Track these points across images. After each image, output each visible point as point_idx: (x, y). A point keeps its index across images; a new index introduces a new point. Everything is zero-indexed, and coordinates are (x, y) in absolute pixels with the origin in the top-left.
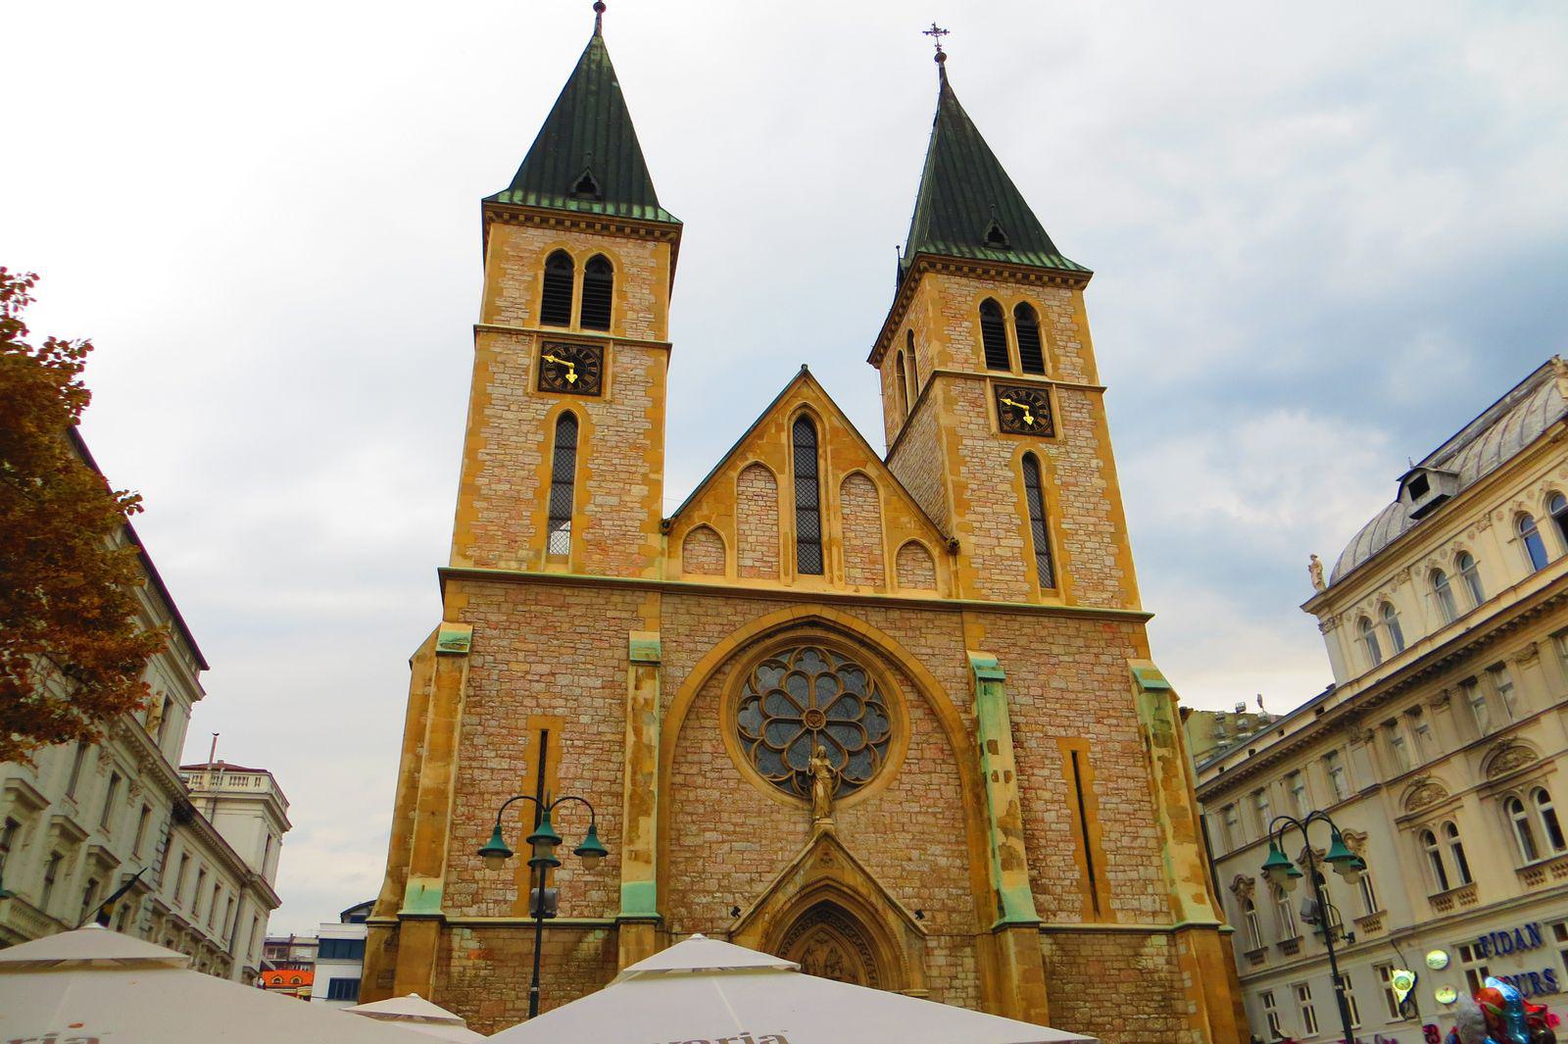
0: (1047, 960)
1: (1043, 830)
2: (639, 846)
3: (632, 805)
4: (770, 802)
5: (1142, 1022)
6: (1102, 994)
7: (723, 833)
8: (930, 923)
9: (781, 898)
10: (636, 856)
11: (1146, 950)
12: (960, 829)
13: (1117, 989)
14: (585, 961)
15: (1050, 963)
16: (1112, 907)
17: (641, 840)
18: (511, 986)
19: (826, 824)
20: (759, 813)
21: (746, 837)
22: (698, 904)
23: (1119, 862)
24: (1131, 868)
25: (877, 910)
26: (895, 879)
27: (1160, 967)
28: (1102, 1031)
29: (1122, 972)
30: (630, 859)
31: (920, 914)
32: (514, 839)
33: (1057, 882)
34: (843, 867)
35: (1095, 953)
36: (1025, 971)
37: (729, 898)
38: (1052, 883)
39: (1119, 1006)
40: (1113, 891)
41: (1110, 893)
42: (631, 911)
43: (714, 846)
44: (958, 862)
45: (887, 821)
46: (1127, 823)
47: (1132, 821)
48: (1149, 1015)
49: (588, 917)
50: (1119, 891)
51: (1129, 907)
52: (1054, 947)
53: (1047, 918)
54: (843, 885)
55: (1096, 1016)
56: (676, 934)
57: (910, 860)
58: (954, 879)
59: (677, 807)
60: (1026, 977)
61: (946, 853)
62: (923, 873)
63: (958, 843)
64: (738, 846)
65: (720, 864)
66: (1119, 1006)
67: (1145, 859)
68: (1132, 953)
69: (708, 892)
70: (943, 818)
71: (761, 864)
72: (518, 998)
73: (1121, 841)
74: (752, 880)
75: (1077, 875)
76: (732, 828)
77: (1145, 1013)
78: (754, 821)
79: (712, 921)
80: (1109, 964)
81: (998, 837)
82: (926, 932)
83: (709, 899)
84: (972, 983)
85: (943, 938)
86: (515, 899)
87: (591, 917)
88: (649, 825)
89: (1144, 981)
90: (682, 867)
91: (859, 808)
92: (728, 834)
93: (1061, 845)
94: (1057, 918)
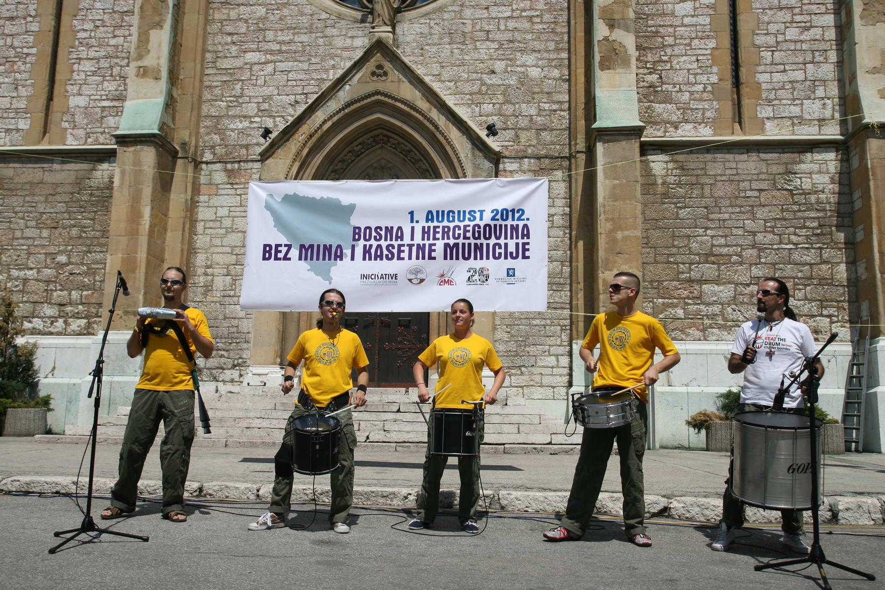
0: (660, 181)
1: (671, 26)
2: (149, 61)
3: (142, 17)
4: (324, 16)
5: (785, 253)
6: (730, 219)
7: (267, 52)
8: (511, 143)
9: (320, 116)
10: (144, 72)
11: (803, 166)
12: (562, 33)
13: (753, 213)
14: (98, 189)
15: (664, 183)
16: (759, 116)
17: (150, 56)
18: (20, 215)
19: (383, 32)
20: (310, 30)
21: (293, 56)
22: (233, 130)
23: (777, 61)
24: (794, 67)
25: (436, 127)
26: (471, 94)
27: (820, 187)
28: (724, 264)
29: (763, 193)
30: (137, 76)
31: (492, 130)
32: (28, 65)
33: (684, 88)
34: (400, 81)
35: (728, 172)
36: (614, 187)
37: (269, 123)
38: (677, 88)
39: (754, 234)
40: (764, 96)
41: (759, 97)
42: (129, 130)
43: (256, 68)
44: (556, 73)
45: (468, 29)
46: (797, 11)
47: (805, 7)
48: (794, 244)
49: (103, 144)
50: (772, 96)
51: (786, 115)
52: (671, 166)
53: (665, 132)
54: (397, 100)
55: (720, 246)
56: (207, 163)
57: (493, 72)
58: (548, 93)
59: (216, 27)
60: (614, 196)
61: (540, 63)
62: (509, 86)
63: (557, 50)
64: (282, 66)
65: (261, 86)
66: (754, 234)
67: (817, 54)
68: (781, 169)
69: (245, 117)
70: (541, 23)
71: (309, 84)
72: (27, 227)
73: (784, 34)
74: (297, 102)
75: (714, 79)
76: (277, 47)
77: (790, 242)
78: (304, 38)
79: (247, 147)
80: (747, 184)
81: (601, 30)
82: (497, 149)
83: (246, 124)
84: (560, 210)
85: (526, 160)
86: (28, 127)
87: (107, 144)
88: (161, 39)
89: (795, 203)
90: (217, 91)
91: (431, 16)
92: (271, 52)
93: (696, 41)
94: (679, 131)
